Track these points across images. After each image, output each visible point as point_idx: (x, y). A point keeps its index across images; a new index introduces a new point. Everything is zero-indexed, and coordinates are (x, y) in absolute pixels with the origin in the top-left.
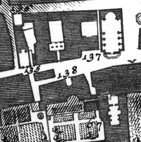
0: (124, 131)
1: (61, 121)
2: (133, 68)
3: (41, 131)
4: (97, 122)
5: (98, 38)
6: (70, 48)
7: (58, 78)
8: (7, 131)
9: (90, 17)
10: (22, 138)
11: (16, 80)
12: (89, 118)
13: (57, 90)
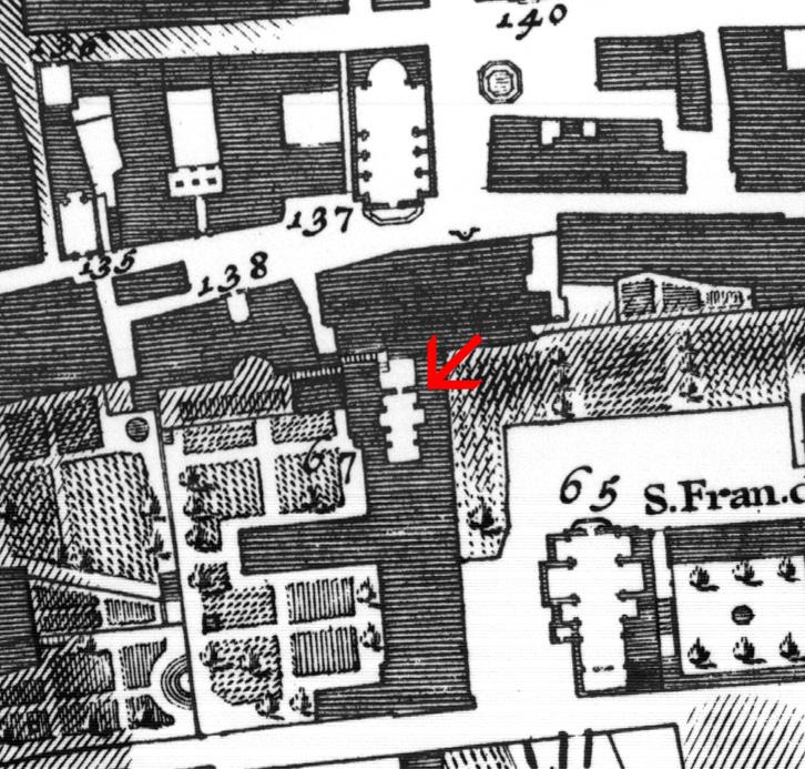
0: (438, 482)
1: (211, 448)
2: (469, 259)
3: (138, 483)
4: (340, 451)
5: (342, 150)
6: (242, 186)
7: (201, 294)
8: (18, 482)
9: (314, 78)
10: (70, 508)
11: (50, 302)
12: (312, 439)
13: (195, 338)
